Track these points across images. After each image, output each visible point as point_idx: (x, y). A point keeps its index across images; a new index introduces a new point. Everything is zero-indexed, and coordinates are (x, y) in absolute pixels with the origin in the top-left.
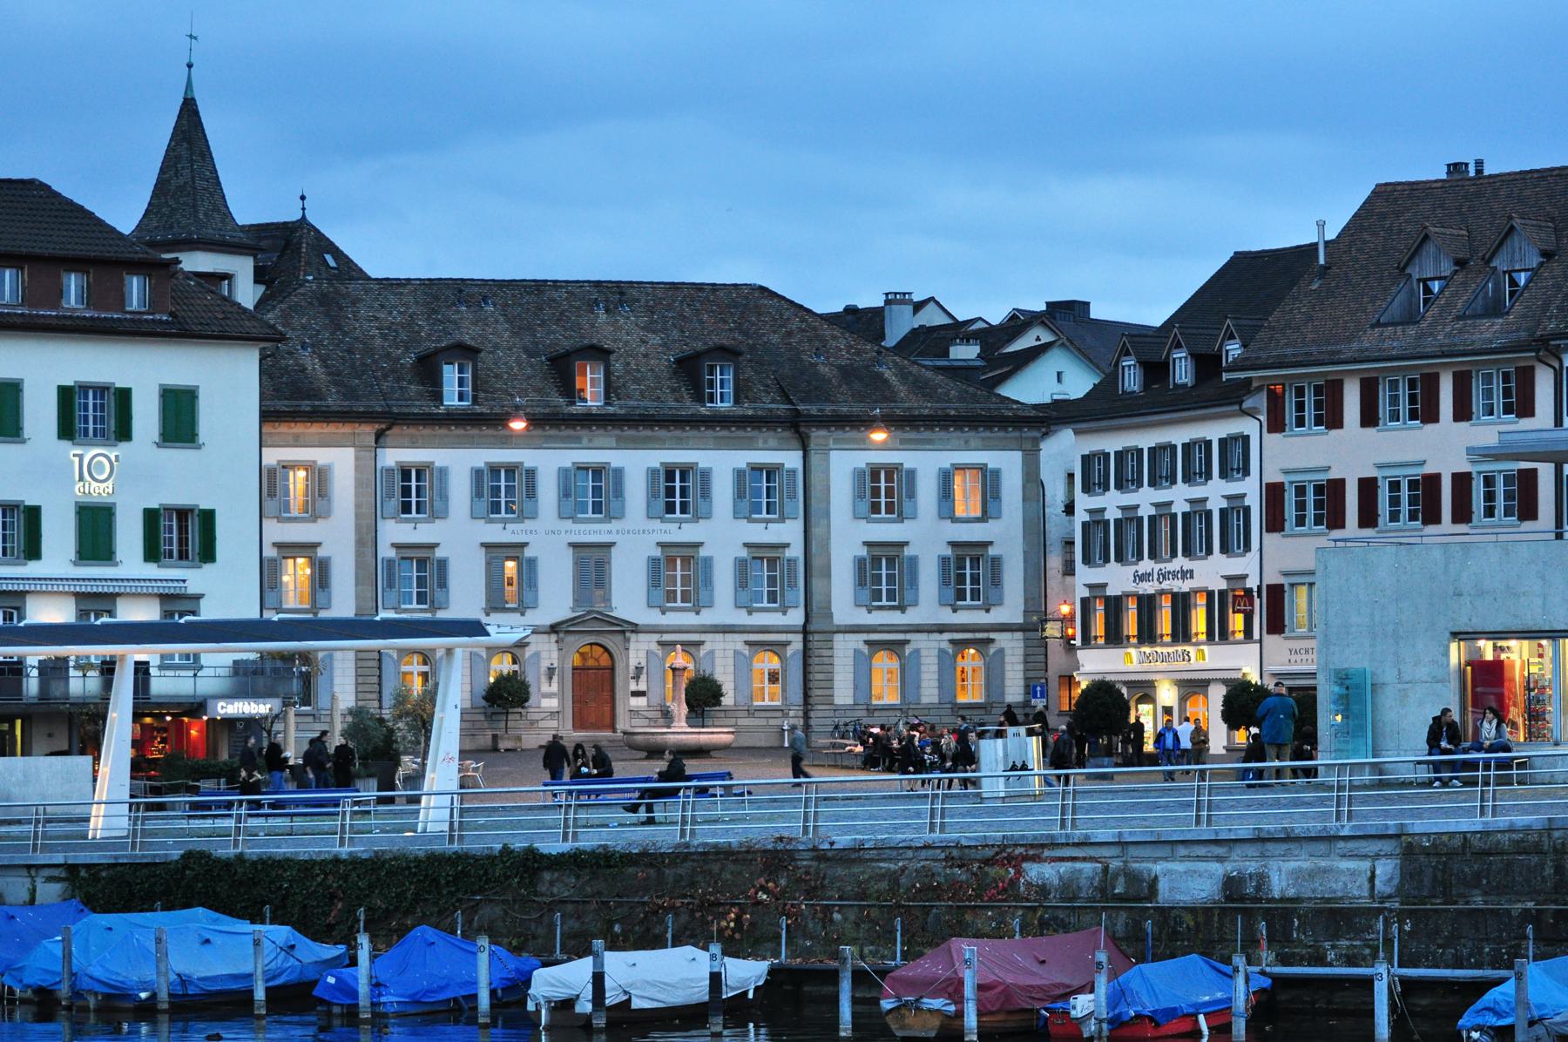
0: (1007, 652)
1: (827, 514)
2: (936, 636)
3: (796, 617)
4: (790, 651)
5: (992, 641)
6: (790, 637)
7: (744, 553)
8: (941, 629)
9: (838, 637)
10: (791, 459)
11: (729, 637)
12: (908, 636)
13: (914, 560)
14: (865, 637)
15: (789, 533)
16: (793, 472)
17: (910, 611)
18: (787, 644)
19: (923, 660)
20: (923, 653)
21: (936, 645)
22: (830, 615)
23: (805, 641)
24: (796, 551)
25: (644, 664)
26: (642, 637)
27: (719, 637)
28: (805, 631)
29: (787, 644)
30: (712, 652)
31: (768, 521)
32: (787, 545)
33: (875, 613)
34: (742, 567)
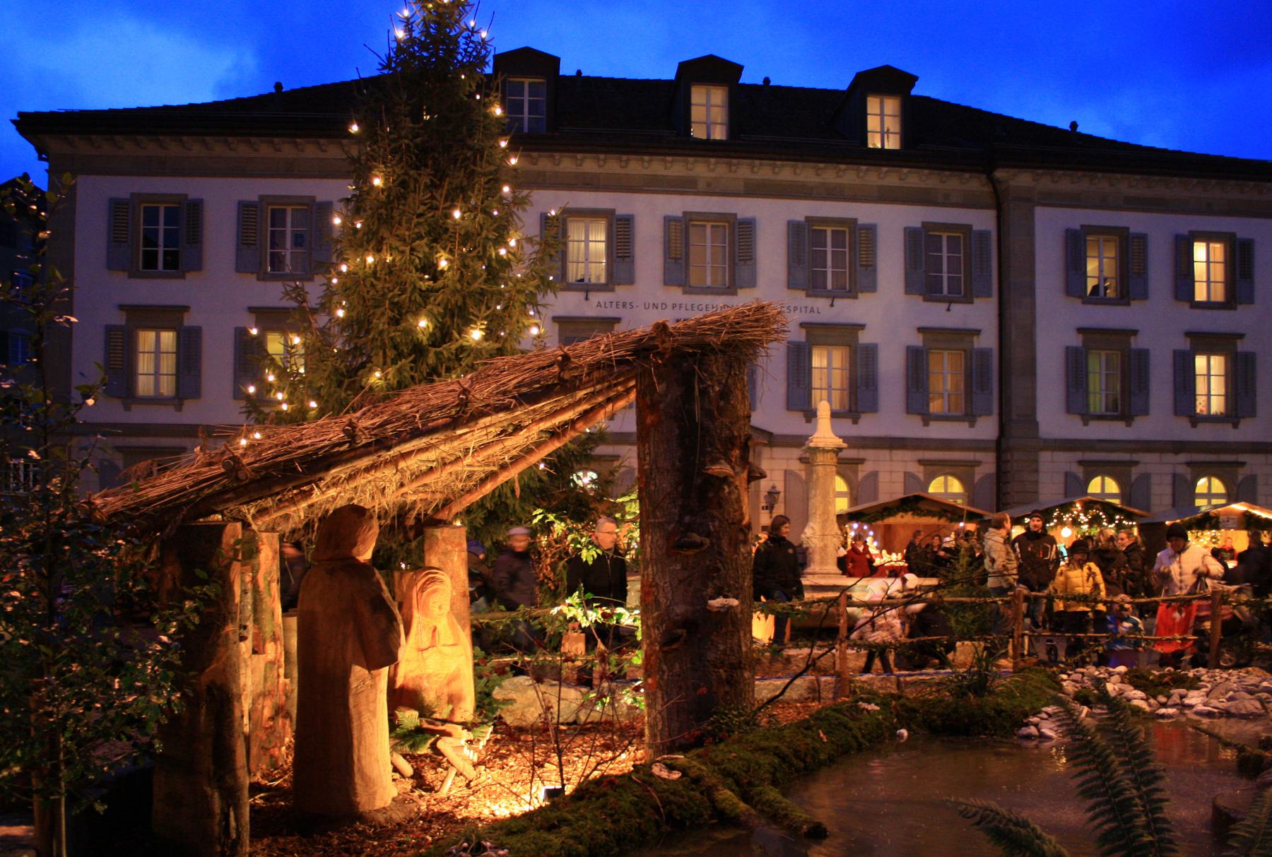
0: (1260, 480)
1: (1031, 290)
2: (1170, 457)
3: (986, 428)
4: (979, 473)
5: (1243, 464)
6: (979, 456)
7: (917, 340)
8: (1178, 447)
9: (1045, 456)
10: (983, 220)
11: (899, 454)
12: (1136, 457)
13: (1143, 355)
14: (1079, 455)
15: (979, 316)
16: (983, 235)
17: (1139, 422)
18: (978, 463)
19: (1156, 490)
20: (1154, 479)
21: (1169, 469)
22: (1036, 424)
23: (999, 462)
24: (988, 340)
25: (780, 487)
26: (778, 452)
27: (884, 454)
28: (1000, 447)
29: (978, 463)
30: (874, 475)
31: (951, 301)
32: (977, 332)
33: (1093, 424)
34: (916, 362)
